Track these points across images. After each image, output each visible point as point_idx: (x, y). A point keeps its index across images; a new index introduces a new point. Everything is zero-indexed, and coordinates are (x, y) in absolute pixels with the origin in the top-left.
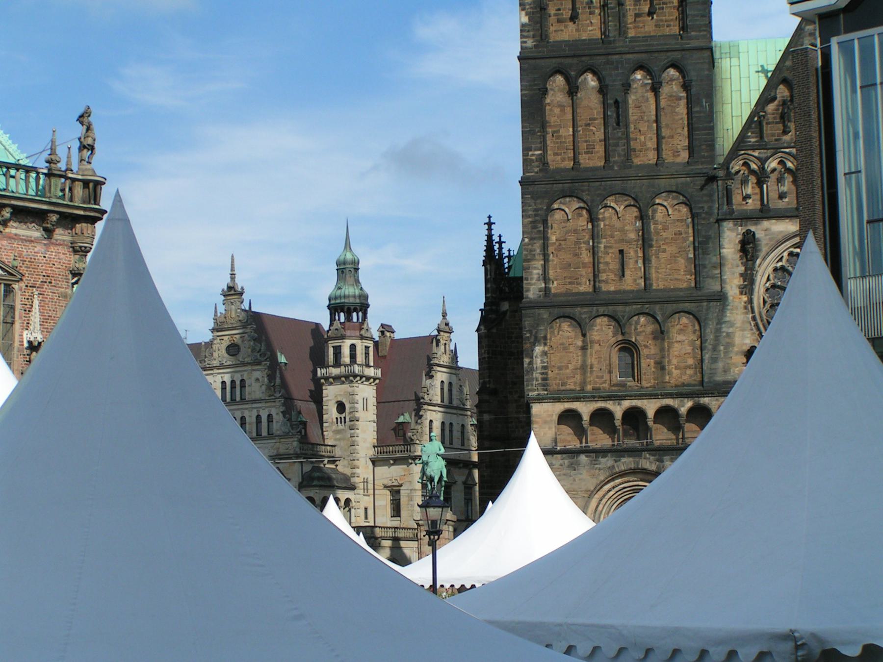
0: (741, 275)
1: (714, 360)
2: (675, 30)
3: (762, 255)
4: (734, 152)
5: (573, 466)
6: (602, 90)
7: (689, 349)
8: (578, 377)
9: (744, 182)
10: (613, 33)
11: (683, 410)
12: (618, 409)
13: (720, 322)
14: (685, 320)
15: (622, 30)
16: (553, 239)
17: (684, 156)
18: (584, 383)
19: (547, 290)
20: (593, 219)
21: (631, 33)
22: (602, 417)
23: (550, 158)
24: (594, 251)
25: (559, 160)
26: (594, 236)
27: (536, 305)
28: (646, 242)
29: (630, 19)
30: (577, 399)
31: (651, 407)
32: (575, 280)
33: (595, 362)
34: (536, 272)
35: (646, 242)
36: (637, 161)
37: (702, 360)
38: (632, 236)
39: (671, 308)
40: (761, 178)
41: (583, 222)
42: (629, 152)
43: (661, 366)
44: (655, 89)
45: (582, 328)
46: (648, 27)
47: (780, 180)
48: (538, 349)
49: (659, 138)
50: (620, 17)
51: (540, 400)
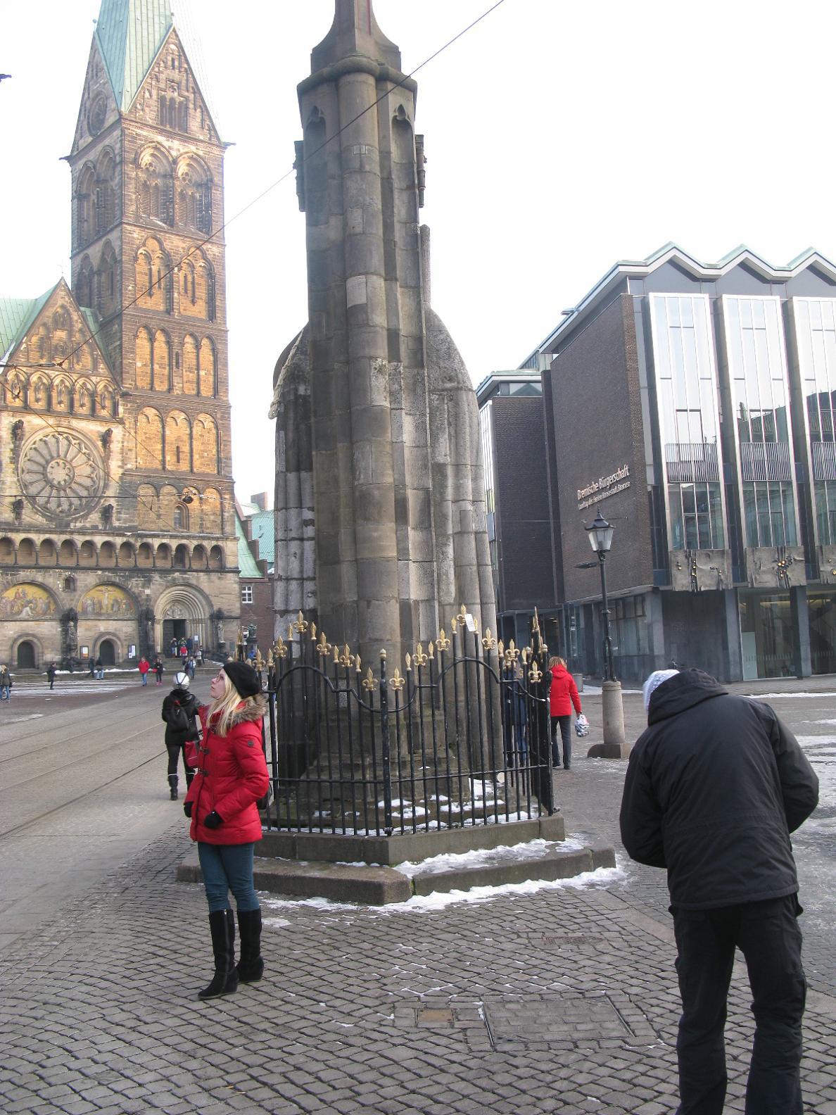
0: (12, 450)
3: (25, 438)
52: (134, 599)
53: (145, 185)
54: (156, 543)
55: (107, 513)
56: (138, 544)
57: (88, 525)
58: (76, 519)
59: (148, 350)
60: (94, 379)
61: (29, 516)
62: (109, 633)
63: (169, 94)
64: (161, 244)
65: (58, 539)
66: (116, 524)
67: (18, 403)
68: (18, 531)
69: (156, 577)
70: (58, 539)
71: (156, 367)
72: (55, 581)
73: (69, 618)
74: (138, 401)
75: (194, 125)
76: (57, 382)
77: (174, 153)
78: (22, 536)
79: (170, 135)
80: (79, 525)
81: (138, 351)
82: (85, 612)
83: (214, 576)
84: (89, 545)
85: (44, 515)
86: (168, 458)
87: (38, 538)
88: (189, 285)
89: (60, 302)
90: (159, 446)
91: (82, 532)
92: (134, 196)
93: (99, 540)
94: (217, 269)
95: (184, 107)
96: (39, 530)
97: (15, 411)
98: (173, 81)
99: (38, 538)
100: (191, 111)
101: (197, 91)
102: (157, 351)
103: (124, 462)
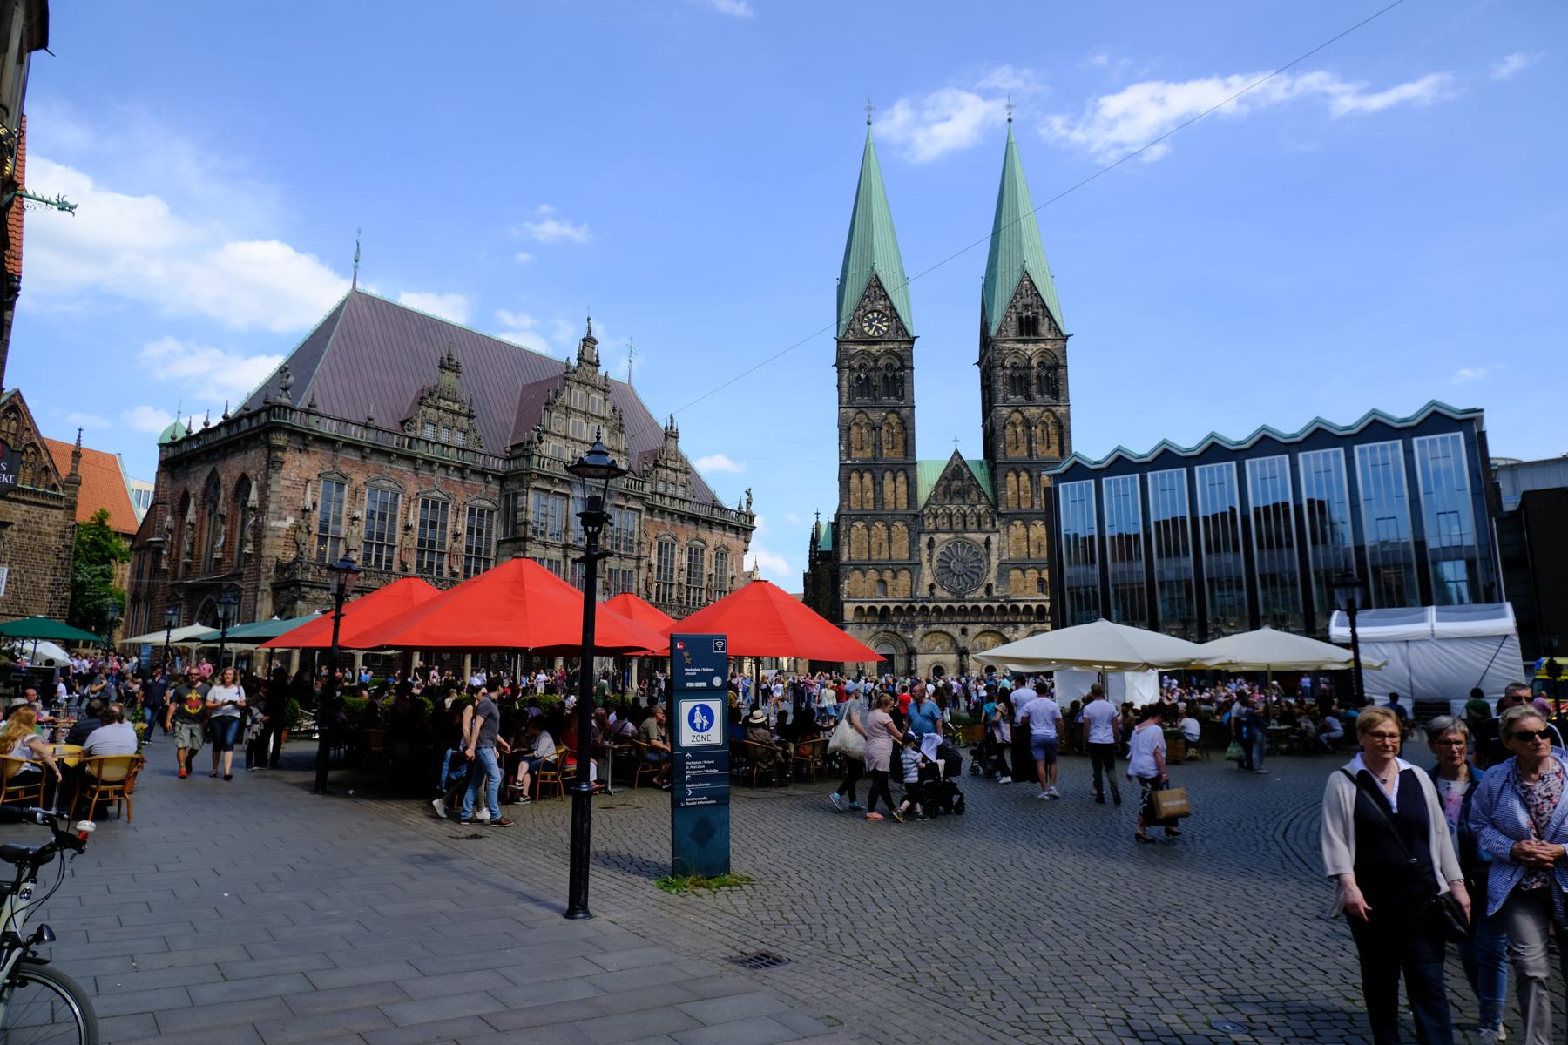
1: (916, 588)
2: (902, 456)
4: (924, 508)
5: (861, 629)
9: (929, 518)
10: (878, 456)
11: (905, 608)
12: (879, 607)
13: (919, 573)
14: (905, 572)
15: (881, 454)
16: (853, 537)
17: (905, 506)
19: (850, 559)
20: (869, 530)
22: (872, 609)
23: (852, 505)
25: (855, 506)
26: (869, 536)
28: (890, 539)
30: (862, 602)
31: (892, 606)
32: (861, 554)
34: (846, 551)
35: (890, 539)
36: (886, 508)
39: (900, 567)
40: (936, 516)
41: (865, 531)
42: (883, 504)
44: (894, 479)
45: (864, 573)
46: (892, 454)
47: (943, 517)
48: (846, 581)
49: (896, 498)
50: (881, 450)
53: (1012, 378)
54: (1021, 605)
55: (989, 589)
56: (1009, 607)
57: (977, 596)
59: (1016, 483)
60: (978, 507)
61: (938, 592)
63: (1025, 314)
64: (1021, 413)
66: (995, 594)
67: (932, 527)
68: (930, 602)
69: (1022, 627)
70: (956, 605)
71: (1022, 493)
72: (955, 630)
73: (963, 653)
74: (1009, 518)
75: (1044, 329)
76: (954, 511)
77: (1029, 353)
78: (934, 604)
79: (1025, 342)
80: (971, 596)
81: (1008, 485)
86: (1031, 550)
87: (943, 606)
88: (1045, 436)
89: (955, 463)
90: (1025, 543)
93: (982, 605)
94: (1064, 422)
97: (929, 533)
99: (943, 606)
100: (1041, 321)
101: (1044, 306)
102: (1022, 483)
103: (1000, 556)
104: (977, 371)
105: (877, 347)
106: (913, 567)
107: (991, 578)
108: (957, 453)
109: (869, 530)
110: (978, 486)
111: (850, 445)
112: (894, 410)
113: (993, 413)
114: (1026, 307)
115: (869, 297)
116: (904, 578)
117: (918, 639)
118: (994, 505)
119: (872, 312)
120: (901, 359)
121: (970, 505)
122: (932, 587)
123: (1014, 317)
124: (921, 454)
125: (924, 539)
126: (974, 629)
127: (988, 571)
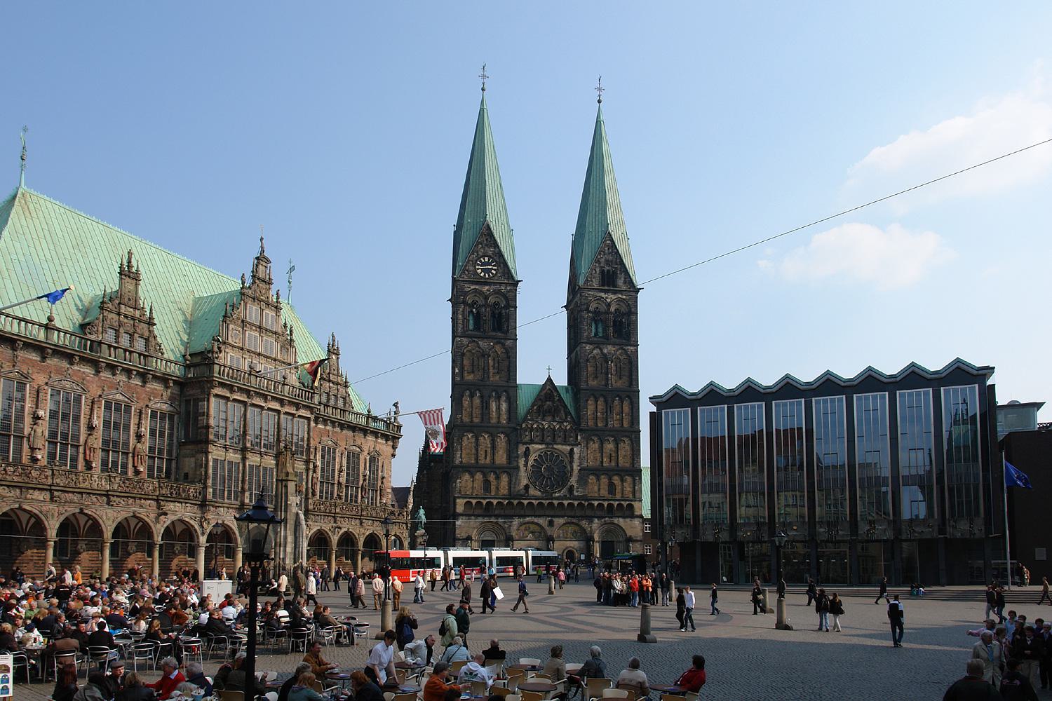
1: (514, 488)
6: (482, 397)
7: (507, 483)
8: (471, 491)
11: (505, 503)
12: (484, 502)
15: (488, 378)
18: (473, 492)
20: (477, 440)
21: (491, 379)
24: (477, 450)
27: (457, 467)
29: (491, 374)
31: (495, 502)
33: (476, 486)
37: (511, 487)
38: (489, 446)
39: (501, 470)
43: (497, 489)
45: (472, 476)
48: (458, 481)
50: (488, 373)
51: (459, 498)
52: (584, 530)
54: (596, 503)
55: (571, 489)
56: (586, 504)
57: (562, 495)
58: (556, 492)
60: (565, 424)
61: (532, 491)
62: (571, 547)
63: (607, 268)
65: (546, 502)
68: (525, 499)
69: (596, 520)
72: (543, 522)
75: (620, 282)
76: (546, 427)
79: (606, 292)
82: (559, 536)
83: (628, 520)
84: (561, 504)
85: (540, 491)
86: (605, 460)
87: (535, 502)
88: (618, 369)
89: (548, 387)
91: (557, 499)
92: (586, 328)
95: (614, 273)
96: (536, 499)
97: (524, 443)
98: (608, 261)
104: (564, 315)
105: (487, 287)
106: (511, 470)
107: (573, 481)
108: (549, 380)
109: (477, 440)
110: (565, 407)
111: (463, 368)
112: (499, 341)
113: (578, 349)
114: (607, 262)
115: (481, 244)
116: (504, 479)
117: (515, 527)
118: (577, 423)
119: (484, 257)
120: (507, 300)
121: (559, 422)
122: (527, 487)
123: (598, 270)
124: (521, 378)
125: (522, 449)
126: (559, 521)
127: (571, 475)
